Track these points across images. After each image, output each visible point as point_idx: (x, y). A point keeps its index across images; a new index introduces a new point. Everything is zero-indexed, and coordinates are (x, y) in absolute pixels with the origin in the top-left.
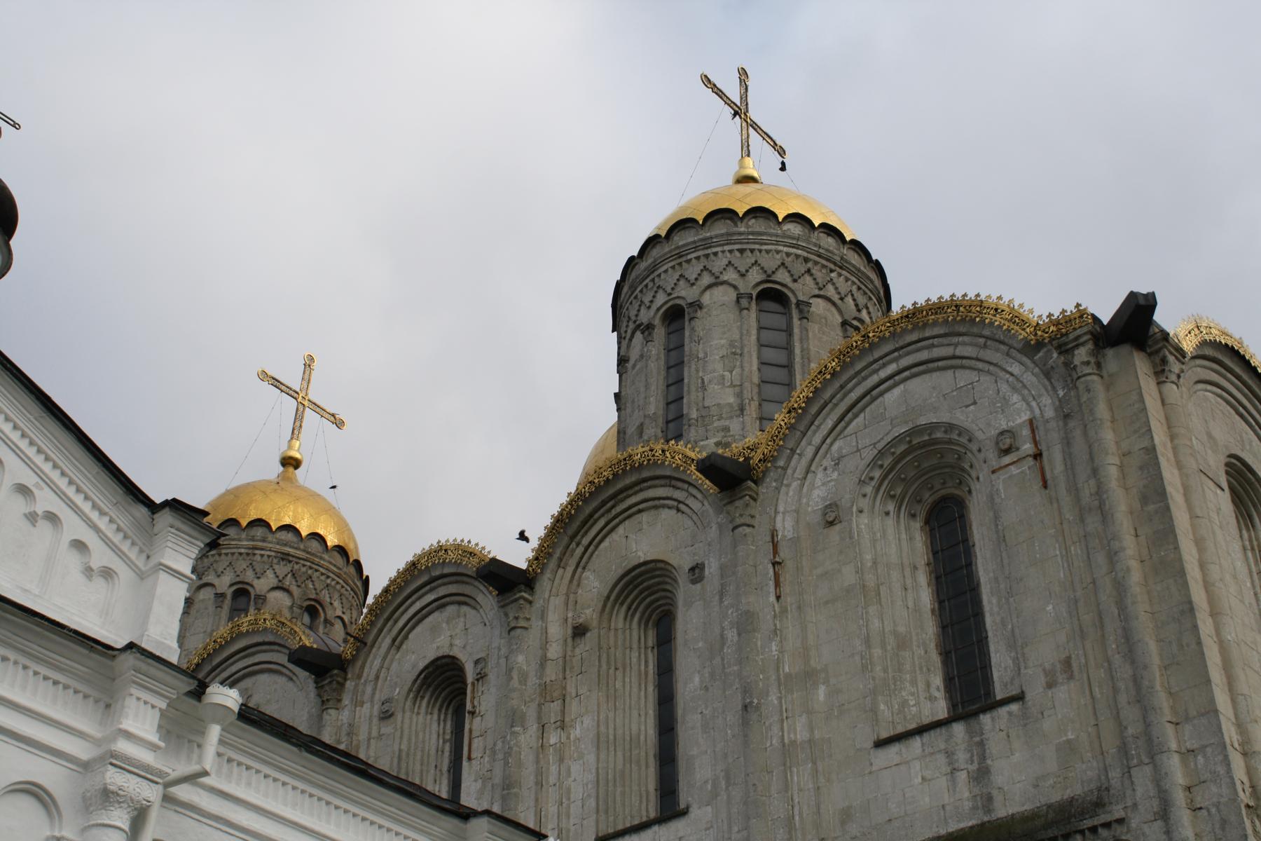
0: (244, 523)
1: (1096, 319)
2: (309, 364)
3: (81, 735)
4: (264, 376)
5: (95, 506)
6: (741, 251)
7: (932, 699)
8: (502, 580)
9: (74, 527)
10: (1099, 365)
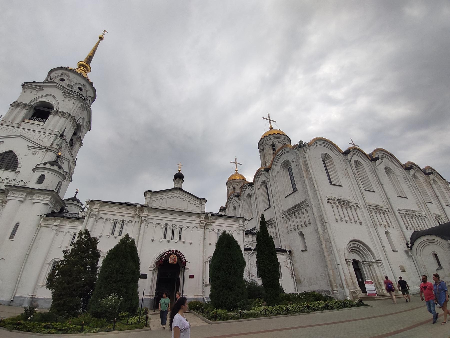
8: (251, 184)
9: (194, 203)
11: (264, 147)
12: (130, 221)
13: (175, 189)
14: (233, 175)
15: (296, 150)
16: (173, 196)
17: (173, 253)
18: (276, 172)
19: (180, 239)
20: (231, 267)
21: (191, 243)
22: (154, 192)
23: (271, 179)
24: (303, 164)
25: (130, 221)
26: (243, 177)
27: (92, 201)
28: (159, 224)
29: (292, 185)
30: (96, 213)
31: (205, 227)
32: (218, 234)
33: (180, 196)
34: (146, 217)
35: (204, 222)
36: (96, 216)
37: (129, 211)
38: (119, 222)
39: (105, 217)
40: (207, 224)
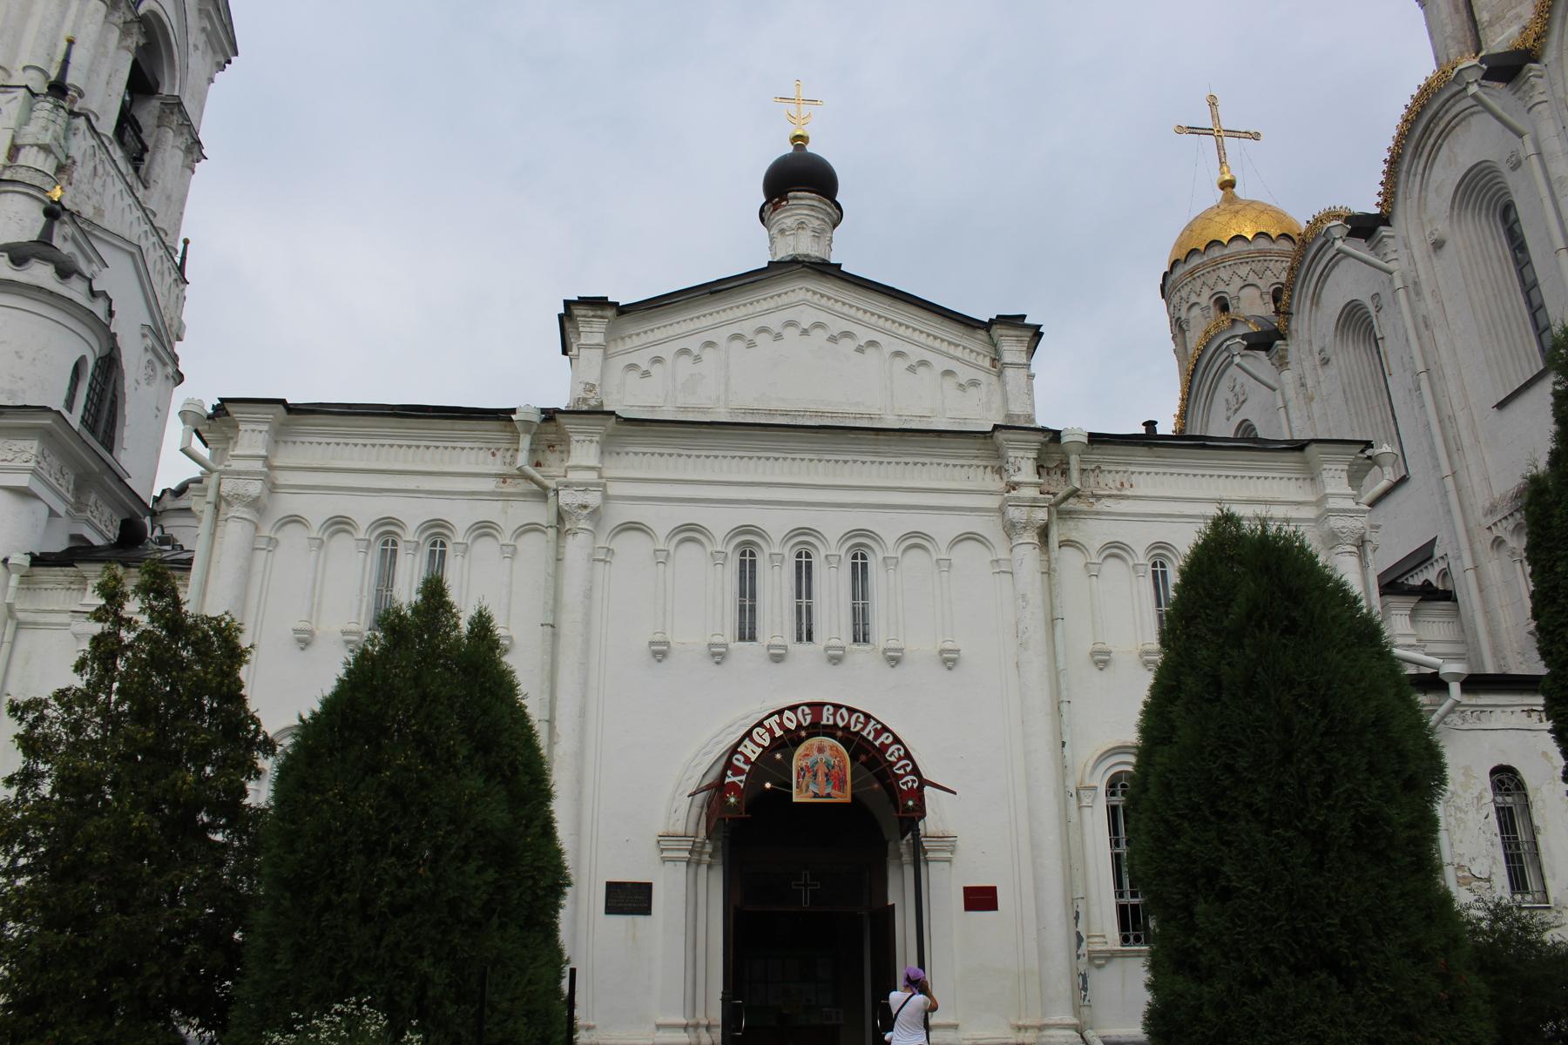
3: (991, 493)
4: (1180, 130)
5: (950, 343)
8: (1364, 227)
12: (484, 529)
13: (779, 270)
14: (1204, 218)
16: (774, 321)
17: (816, 729)
19: (861, 634)
21: (950, 660)
22: (623, 311)
25: (484, 529)
26: (1279, 216)
27: (223, 408)
28: (690, 533)
30: (255, 488)
31: (1044, 533)
32: (1159, 578)
33: (823, 317)
34: (585, 487)
35: (1032, 492)
36: (255, 504)
37: (471, 458)
38: (410, 534)
39: (317, 509)
40: (1060, 511)
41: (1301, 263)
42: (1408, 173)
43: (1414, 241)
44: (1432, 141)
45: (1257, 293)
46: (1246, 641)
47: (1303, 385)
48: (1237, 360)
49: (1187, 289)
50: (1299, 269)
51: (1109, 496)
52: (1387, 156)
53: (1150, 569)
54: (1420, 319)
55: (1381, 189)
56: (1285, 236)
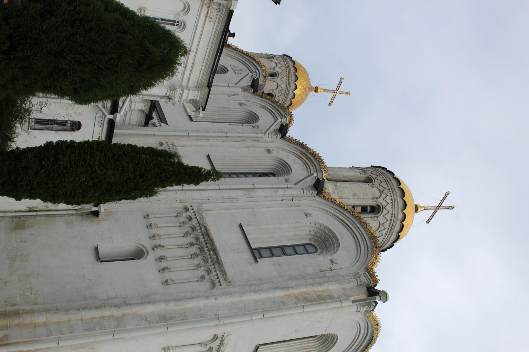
0: (296, 74)
1: (376, 285)
2: (347, 93)
4: (342, 79)
6: (391, 199)
7: (255, 243)
8: (283, 130)
10: (360, 285)
11: (376, 184)
14: (307, 77)
15: (363, 279)
18: (309, 210)
20: (79, 62)
23: (294, 192)
24: (324, 291)
26: (299, 104)
29: (270, 249)
32: (172, 22)
41: (278, 106)
42: (296, 148)
43: (273, 144)
44: (304, 158)
45: (274, 88)
46: (138, 47)
47: (235, 95)
48: (250, 74)
49: (283, 64)
50: (276, 104)
51: (208, 12)
52: (304, 144)
53: (177, 20)
54: (245, 139)
55: (294, 139)
56: (291, 104)
